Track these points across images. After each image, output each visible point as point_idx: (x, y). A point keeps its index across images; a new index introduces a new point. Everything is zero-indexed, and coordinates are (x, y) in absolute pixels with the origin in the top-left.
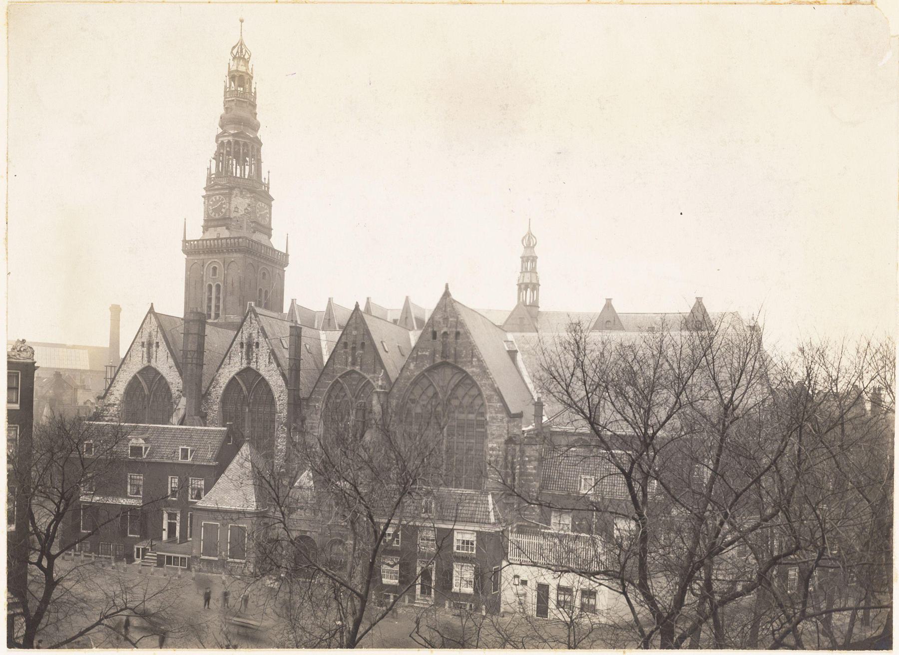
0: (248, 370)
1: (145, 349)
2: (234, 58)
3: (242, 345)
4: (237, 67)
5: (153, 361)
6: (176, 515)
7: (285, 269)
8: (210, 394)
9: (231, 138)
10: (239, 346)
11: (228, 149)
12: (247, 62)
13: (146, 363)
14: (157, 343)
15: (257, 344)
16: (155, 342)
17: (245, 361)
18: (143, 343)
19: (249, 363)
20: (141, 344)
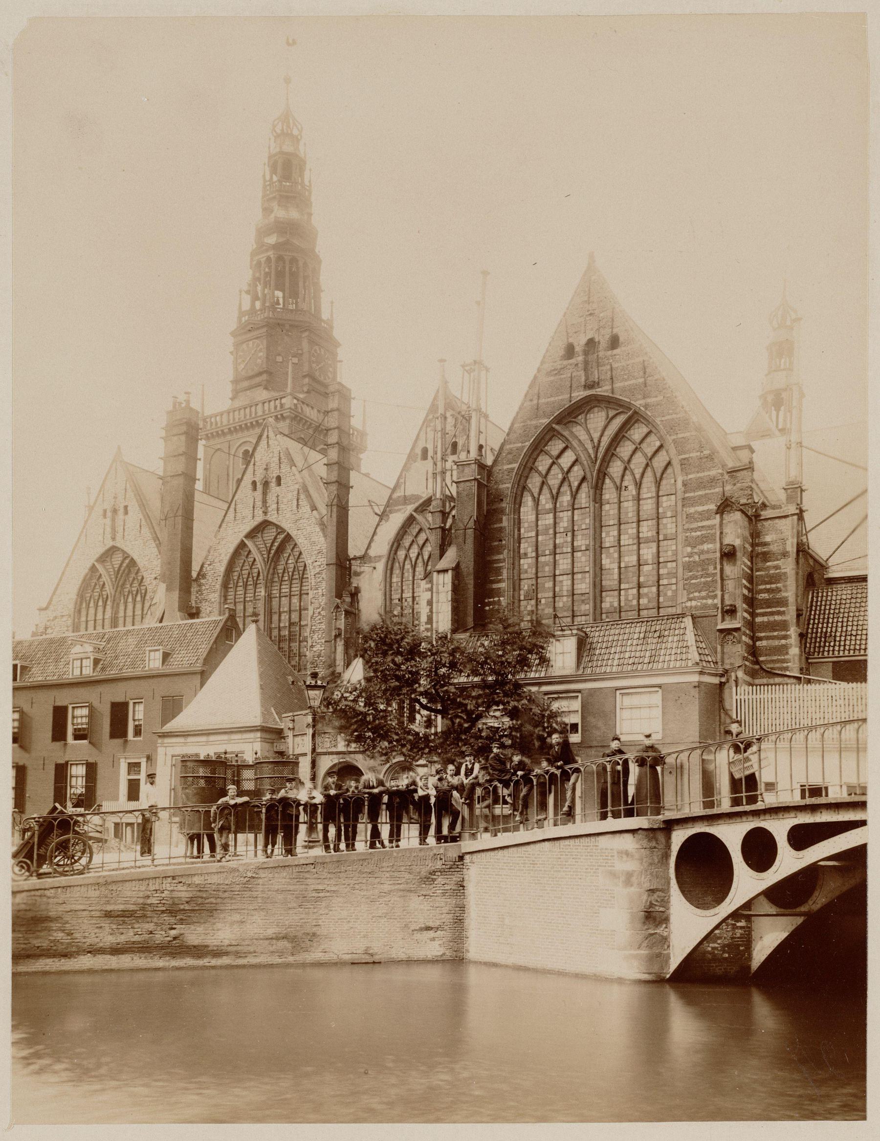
0: (264, 525)
1: (108, 521)
2: (277, 136)
3: (254, 483)
4: (281, 148)
5: (119, 536)
6: (138, 765)
7: (361, 456)
8: (204, 576)
9: (271, 253)
10: (250, 486)
11: (267, 270)
12: (296, 140)
13: (110, 543)
14: (126, 507)
15: (279, 479)
16: (122, 506)
17: (259, 513)
18: (105, 511)
19: (265, 513)
20: (101, 512)
